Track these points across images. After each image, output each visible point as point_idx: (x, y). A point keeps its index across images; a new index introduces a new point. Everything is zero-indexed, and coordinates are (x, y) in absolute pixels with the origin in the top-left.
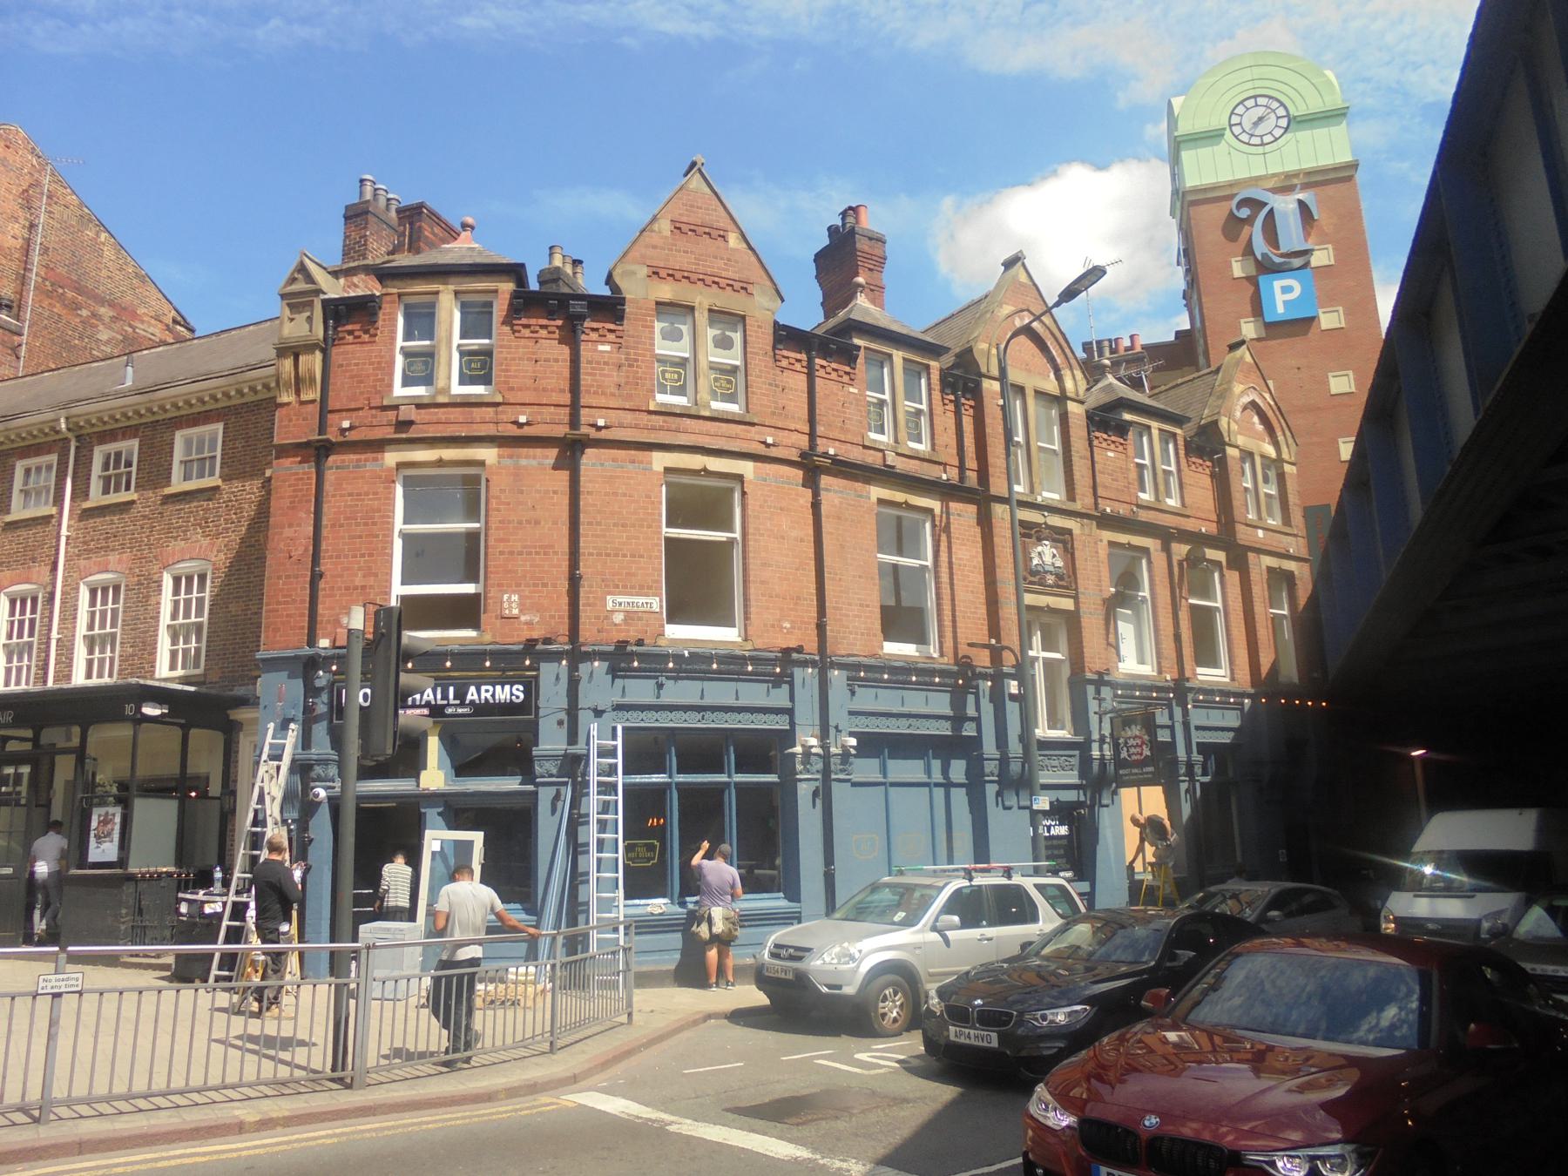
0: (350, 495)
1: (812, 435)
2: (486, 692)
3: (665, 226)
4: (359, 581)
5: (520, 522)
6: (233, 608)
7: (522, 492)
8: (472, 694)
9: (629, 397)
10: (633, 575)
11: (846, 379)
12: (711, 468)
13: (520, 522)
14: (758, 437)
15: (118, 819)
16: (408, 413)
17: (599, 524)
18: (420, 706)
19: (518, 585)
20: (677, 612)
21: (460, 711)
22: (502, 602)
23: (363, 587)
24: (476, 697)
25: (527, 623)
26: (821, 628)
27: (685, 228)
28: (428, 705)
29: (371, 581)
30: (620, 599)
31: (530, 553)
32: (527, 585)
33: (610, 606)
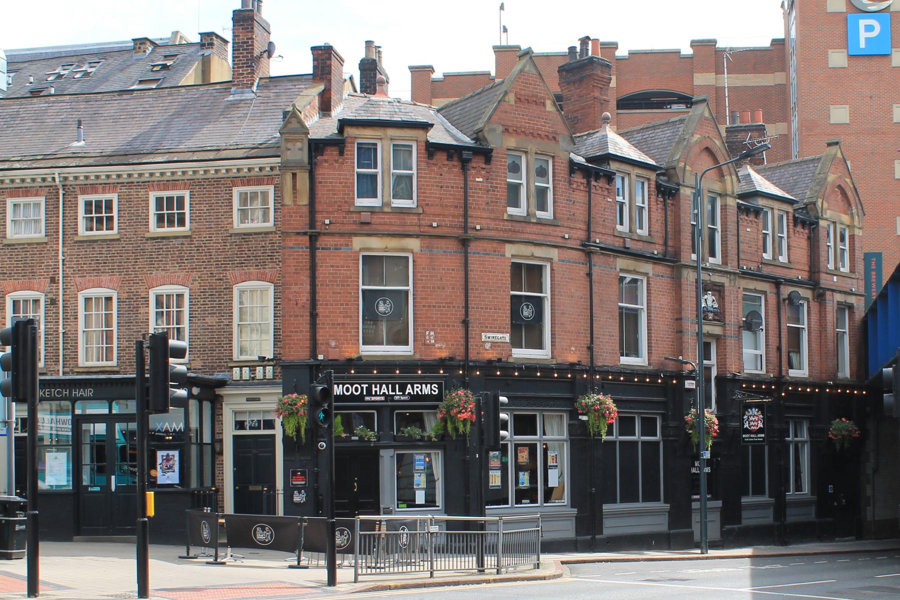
0: (332, 266)
1: (588, 230)
2: (417, 389)
3: (511, 98)
4: (340, 320)
5: (434, 288)
6: (210, 320)
7: (434, 269)
8: (409, 389)
9: (493, 211)
10: (496, 320)
11: (606, 193)
12: (536, 255)
13: (434, 288)
14: (560, 234)
15: (177, 458)
16: (366, 217)
17: (477, 289)
18: (380, 395)
19: (434, 326)
20: (516, 342)
21: (402, 398)
22: (425, 336)
23: (343, 324)
24: (411, 391)
25: (439, 348)
26: (590, 349)
27: (523, 98)
28: (384, 394)
29: (348, 320)
30: (489, 335)
31: (439, 307)
32: (439, 326)
33: (483, 339)
